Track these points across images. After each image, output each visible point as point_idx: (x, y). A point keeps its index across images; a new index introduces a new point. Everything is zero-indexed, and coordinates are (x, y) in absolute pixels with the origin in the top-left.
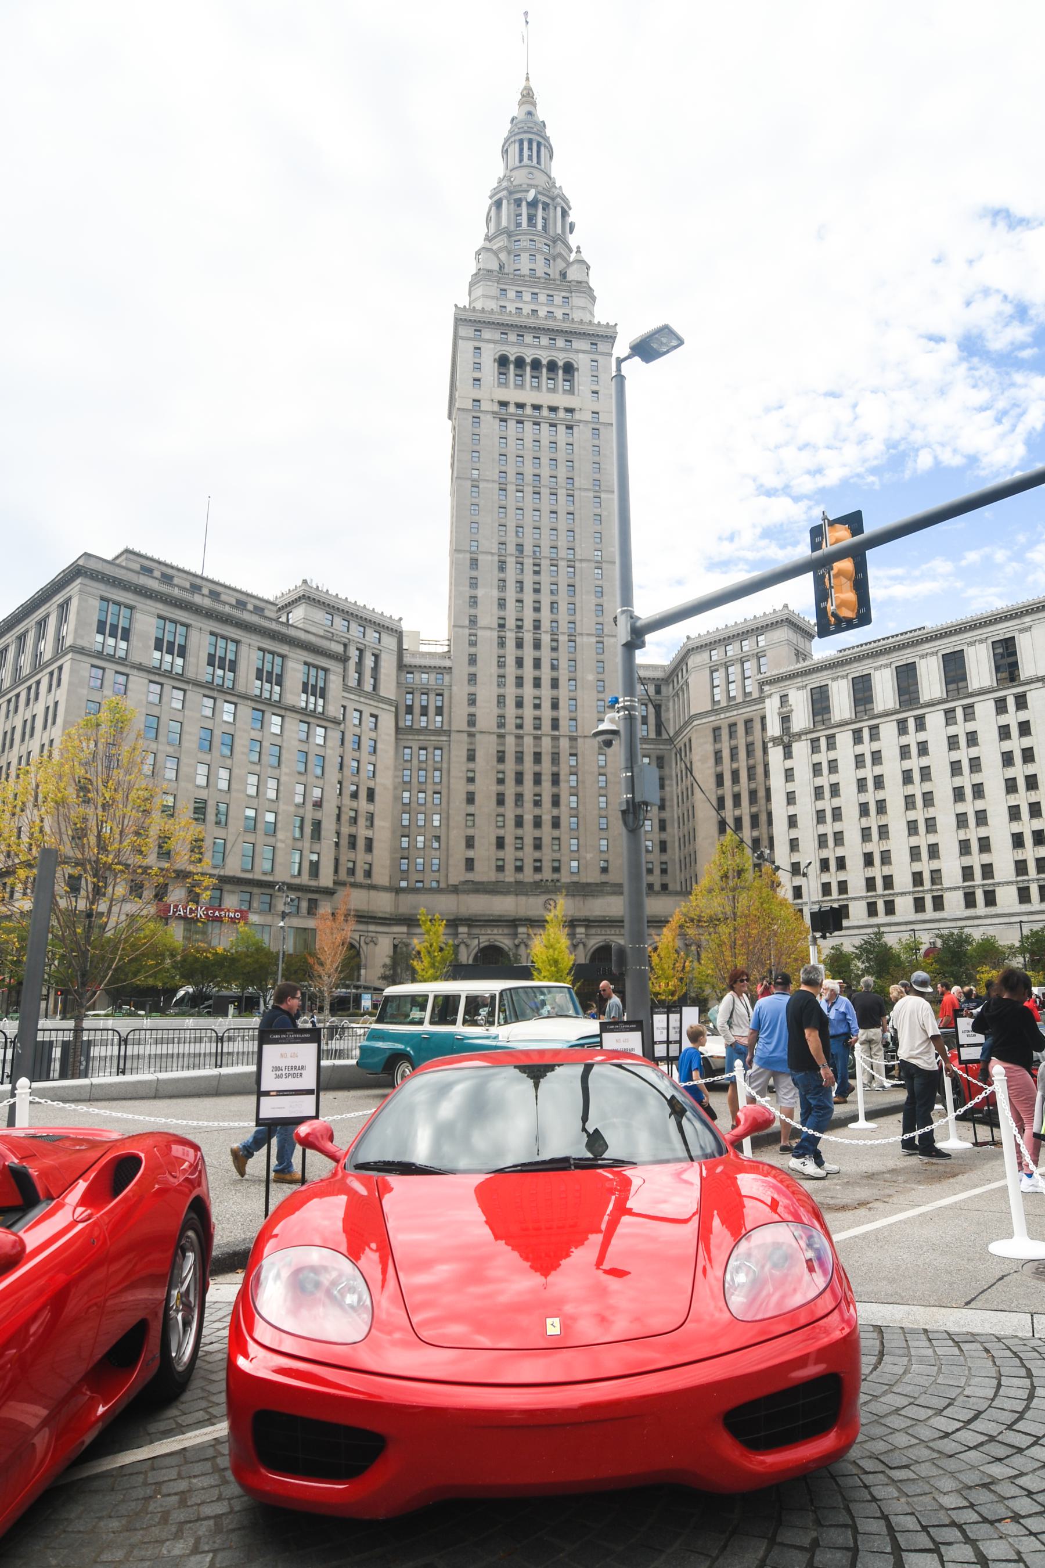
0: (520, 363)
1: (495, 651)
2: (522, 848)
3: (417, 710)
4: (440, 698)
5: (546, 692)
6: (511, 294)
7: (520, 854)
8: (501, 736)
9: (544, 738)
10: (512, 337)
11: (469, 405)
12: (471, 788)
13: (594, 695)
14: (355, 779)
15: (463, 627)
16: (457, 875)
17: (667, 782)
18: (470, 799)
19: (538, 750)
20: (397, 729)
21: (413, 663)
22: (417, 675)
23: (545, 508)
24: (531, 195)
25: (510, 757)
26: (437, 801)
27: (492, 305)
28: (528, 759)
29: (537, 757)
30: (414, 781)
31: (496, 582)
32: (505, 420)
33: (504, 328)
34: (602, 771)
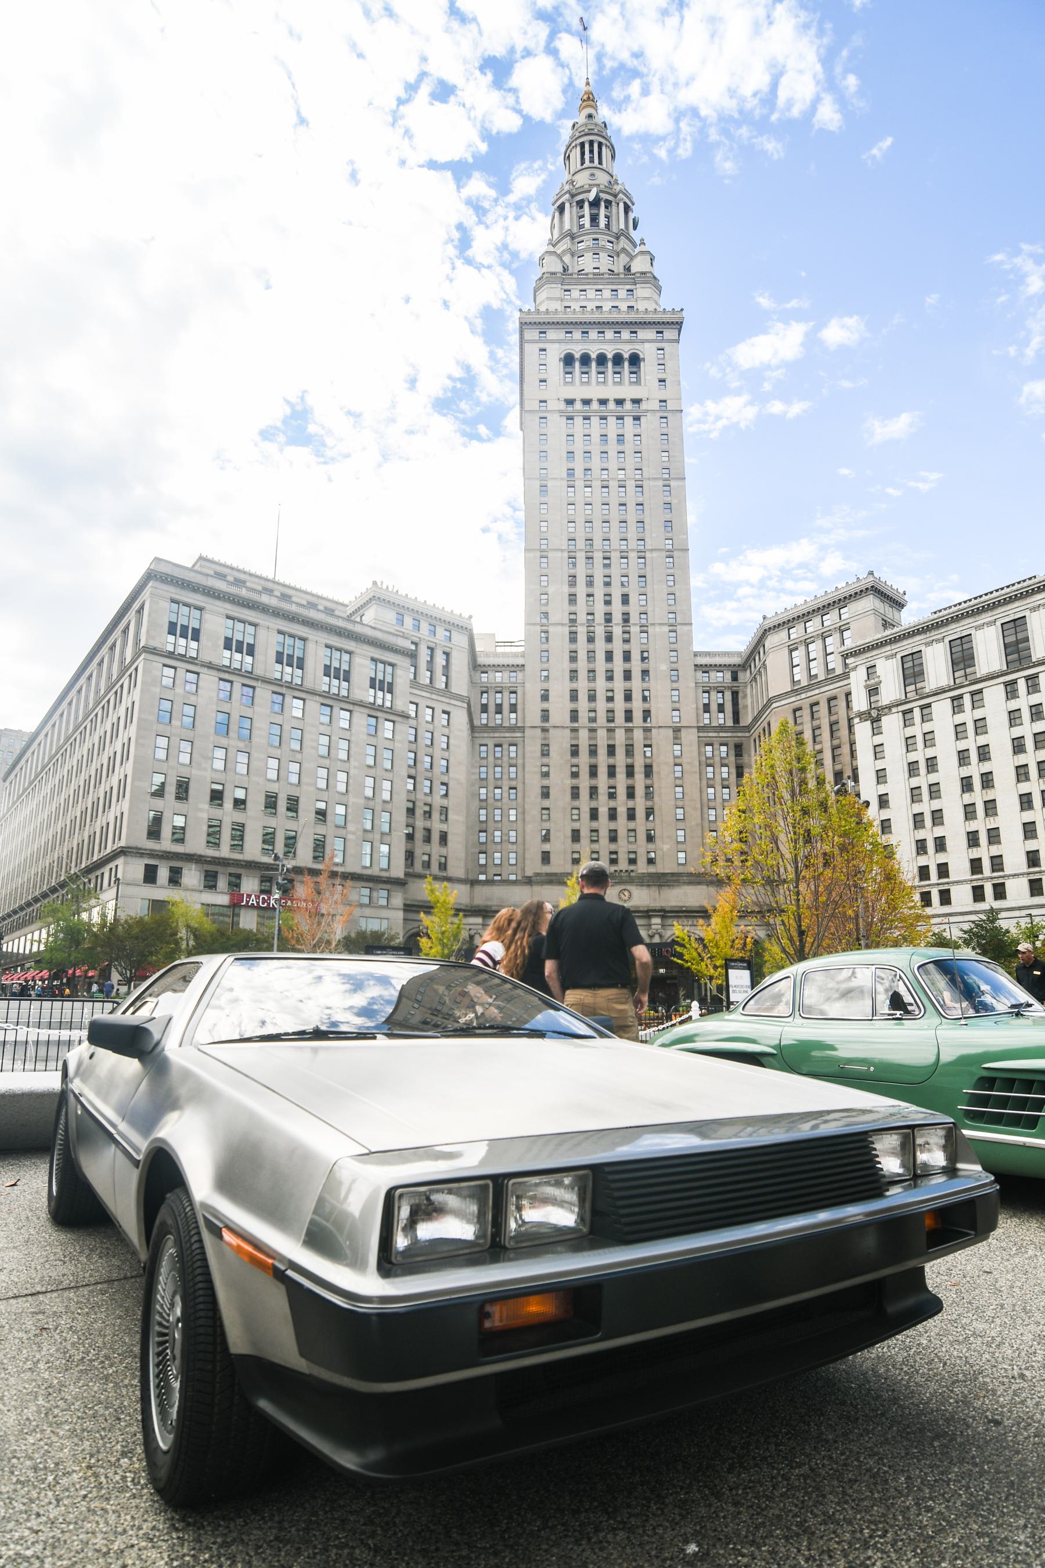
0: (585, 360)
1: (567, 646)
2: (597, 841)
3: (492, 708)
4: (514, 695)
5: (619, 685)
6: (576, 293)
7: (595, 847)
8: (575, 730)
9: (617, 730)
10: (577, 335)
11: (535, 405)
12: (546, 782)
13: (668, 685)
14: (429, 775)
15: (535, 624)
16: (533, 866)
17: (746, 770)
18: (546, 794)
19: (611, 742)
20: (473, 728)
21: (487, 663)
22: (491, 674)
23: (614, 502)
24: (594, 191)
25: (584, 751)
26: (513, 797)
27: (558, 306)
28: (602, 752)
29: (611, 750)
30: (491, 777)
31: (566, 579)
33: (568, 326)
34: (678, 761)
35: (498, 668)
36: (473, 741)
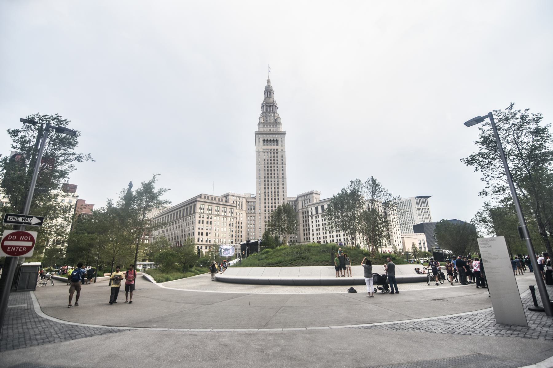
0: (267, 140)
20: (247, 214)
35: (251, 202)
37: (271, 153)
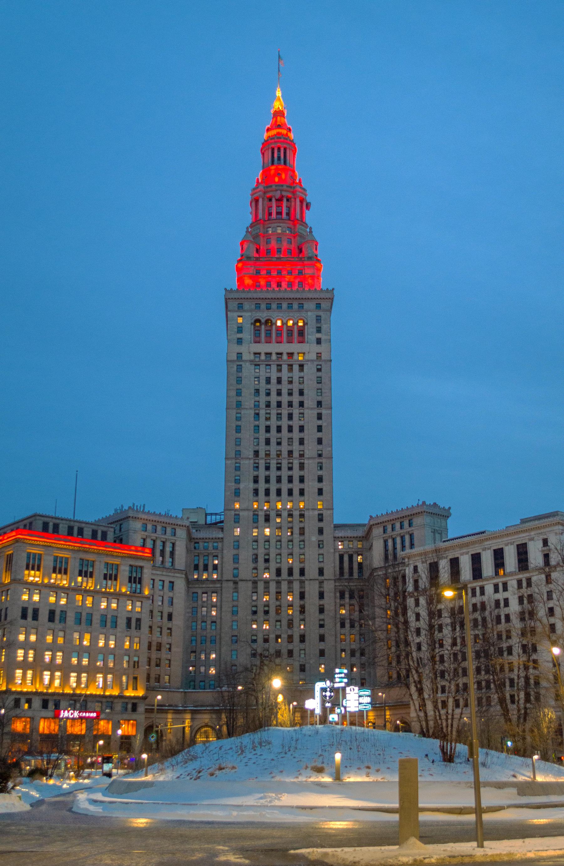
8: (255, 583)
9: (283, 582)
10: (263, 306)
20: (189, 582)
26: (213, 628)
32: (259, 365)
36: (188, 587)
37: (279, 370)
